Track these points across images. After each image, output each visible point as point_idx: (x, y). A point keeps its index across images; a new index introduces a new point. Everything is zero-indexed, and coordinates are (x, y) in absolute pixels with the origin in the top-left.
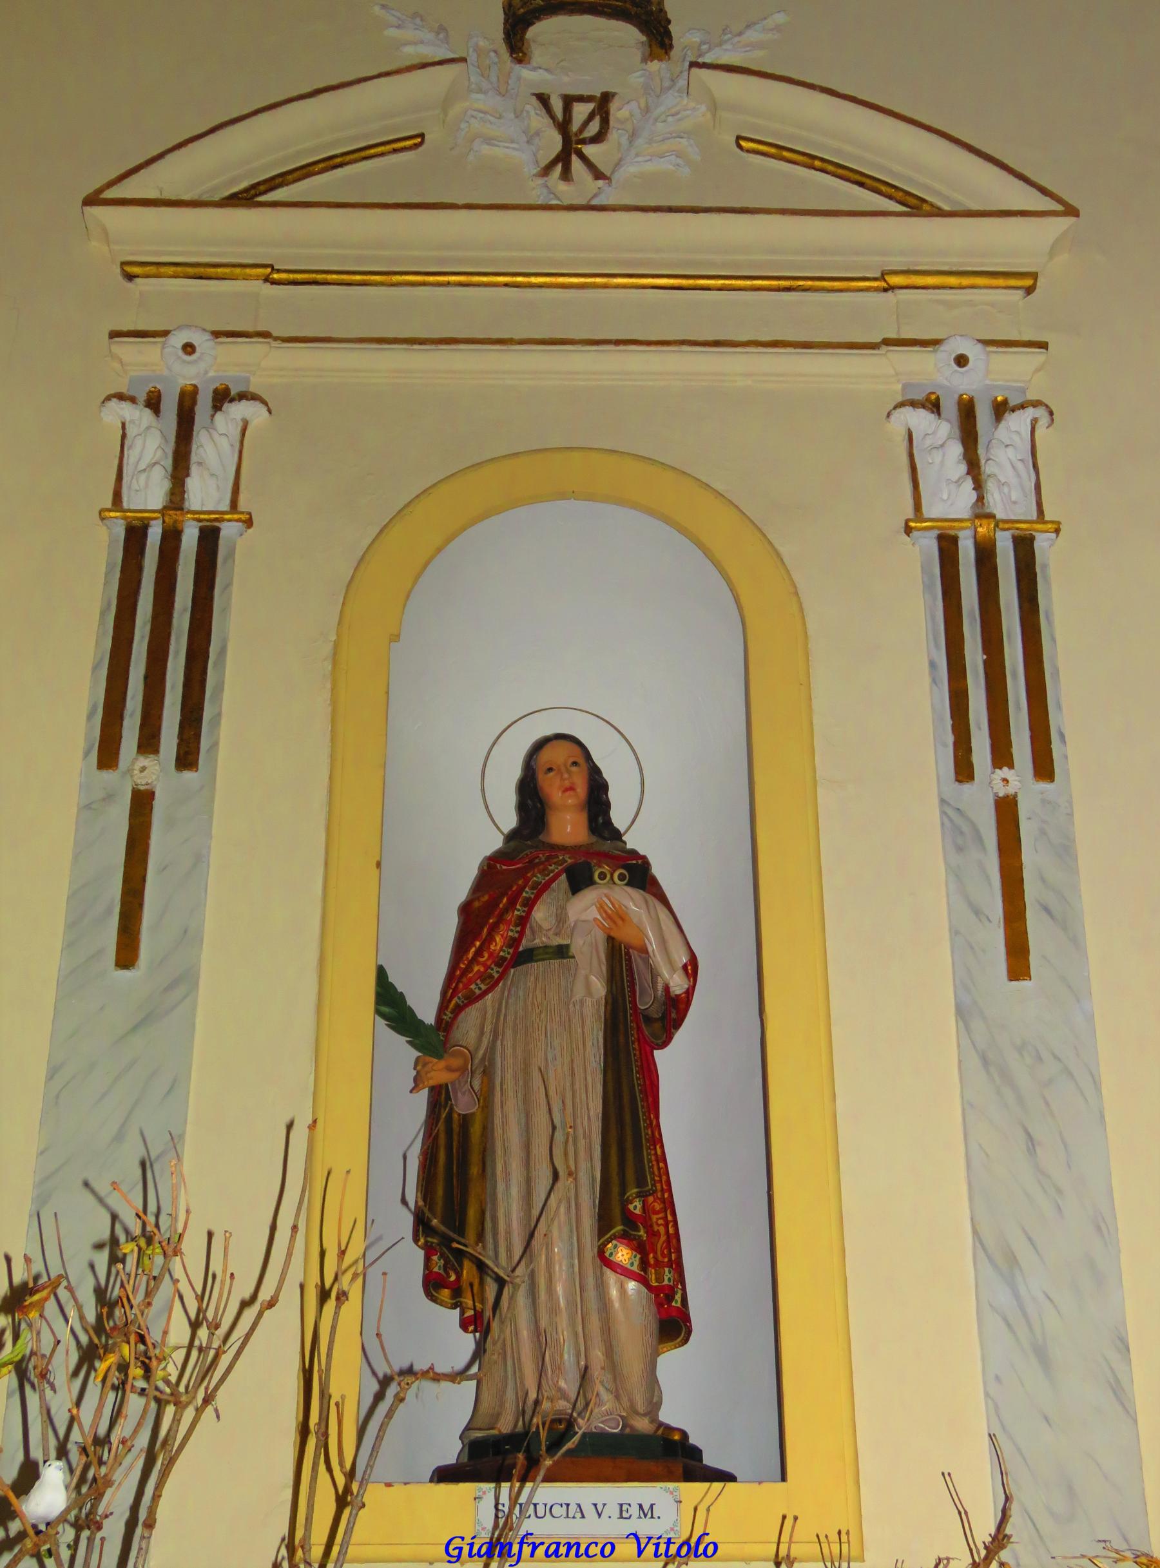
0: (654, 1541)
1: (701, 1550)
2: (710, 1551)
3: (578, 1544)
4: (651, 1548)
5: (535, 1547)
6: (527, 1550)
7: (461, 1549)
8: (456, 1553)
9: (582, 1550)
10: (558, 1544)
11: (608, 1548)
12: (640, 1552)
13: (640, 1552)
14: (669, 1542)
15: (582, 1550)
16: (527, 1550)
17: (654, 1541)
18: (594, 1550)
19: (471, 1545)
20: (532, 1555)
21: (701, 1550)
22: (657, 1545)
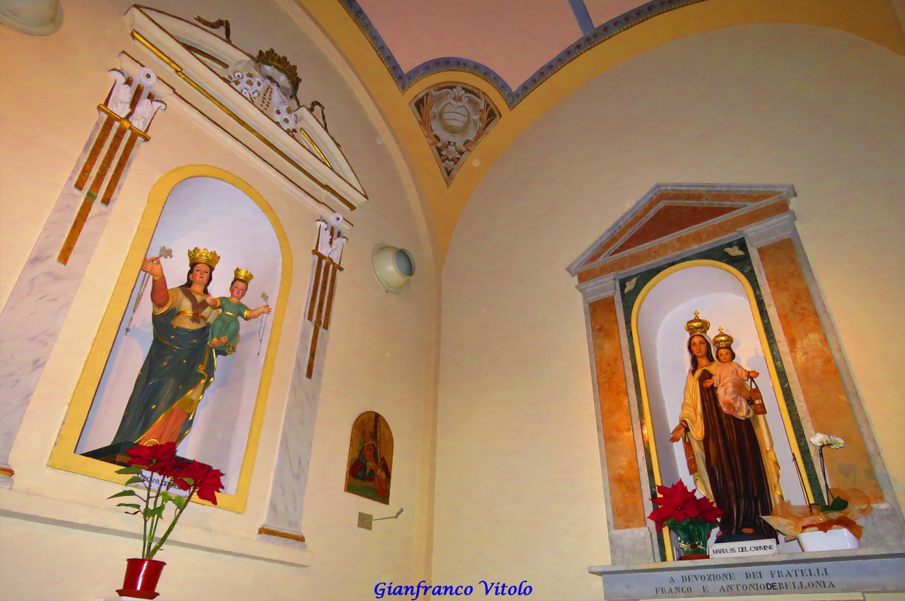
0: (495, 585)
1: (522, 591)
2: (528, 589)
3: (451, 587)
4: (493, 590)
5: (426, 589)
6: (422, 590)
7: (384, 590)
8: (381, 592)
9: (454, 591)
10: (401, 587)
11: (469, 590)
12: (487, 592)
13: (487, 592)
14: (504, 586)
15: (454, 591)
16: (422, 590)
17: (495, 585)
18: (460, 591)
19: (390, 588)
20: (425, 594)
21: (522, 591)
22: (497, 588)
